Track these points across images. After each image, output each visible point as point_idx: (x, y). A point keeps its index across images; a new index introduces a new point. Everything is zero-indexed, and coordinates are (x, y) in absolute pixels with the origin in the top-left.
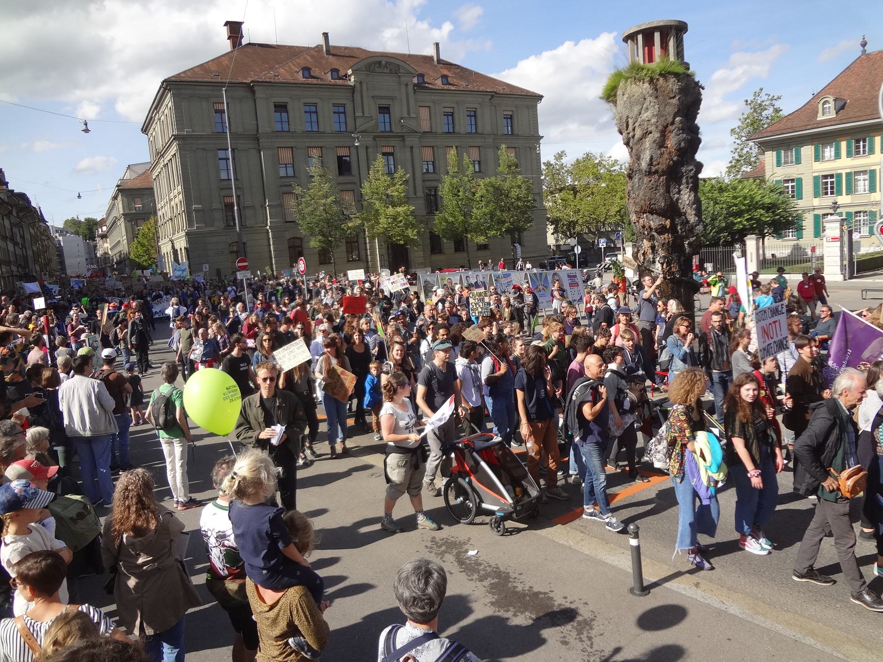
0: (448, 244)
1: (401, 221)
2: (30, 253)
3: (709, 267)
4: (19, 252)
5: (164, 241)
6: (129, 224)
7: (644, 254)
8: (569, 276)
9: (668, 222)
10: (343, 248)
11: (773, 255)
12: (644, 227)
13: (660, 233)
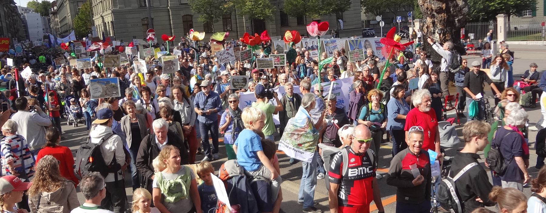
0: (293, 20)
1: (261, 4)
3: (472, 36)
6: (72, 5)
7: (427, 27)
8: (376, 42)
9: (444, 6)
10: (221, 22)
11: (516, 28)
12: (427, 9)
13: (438, 13)
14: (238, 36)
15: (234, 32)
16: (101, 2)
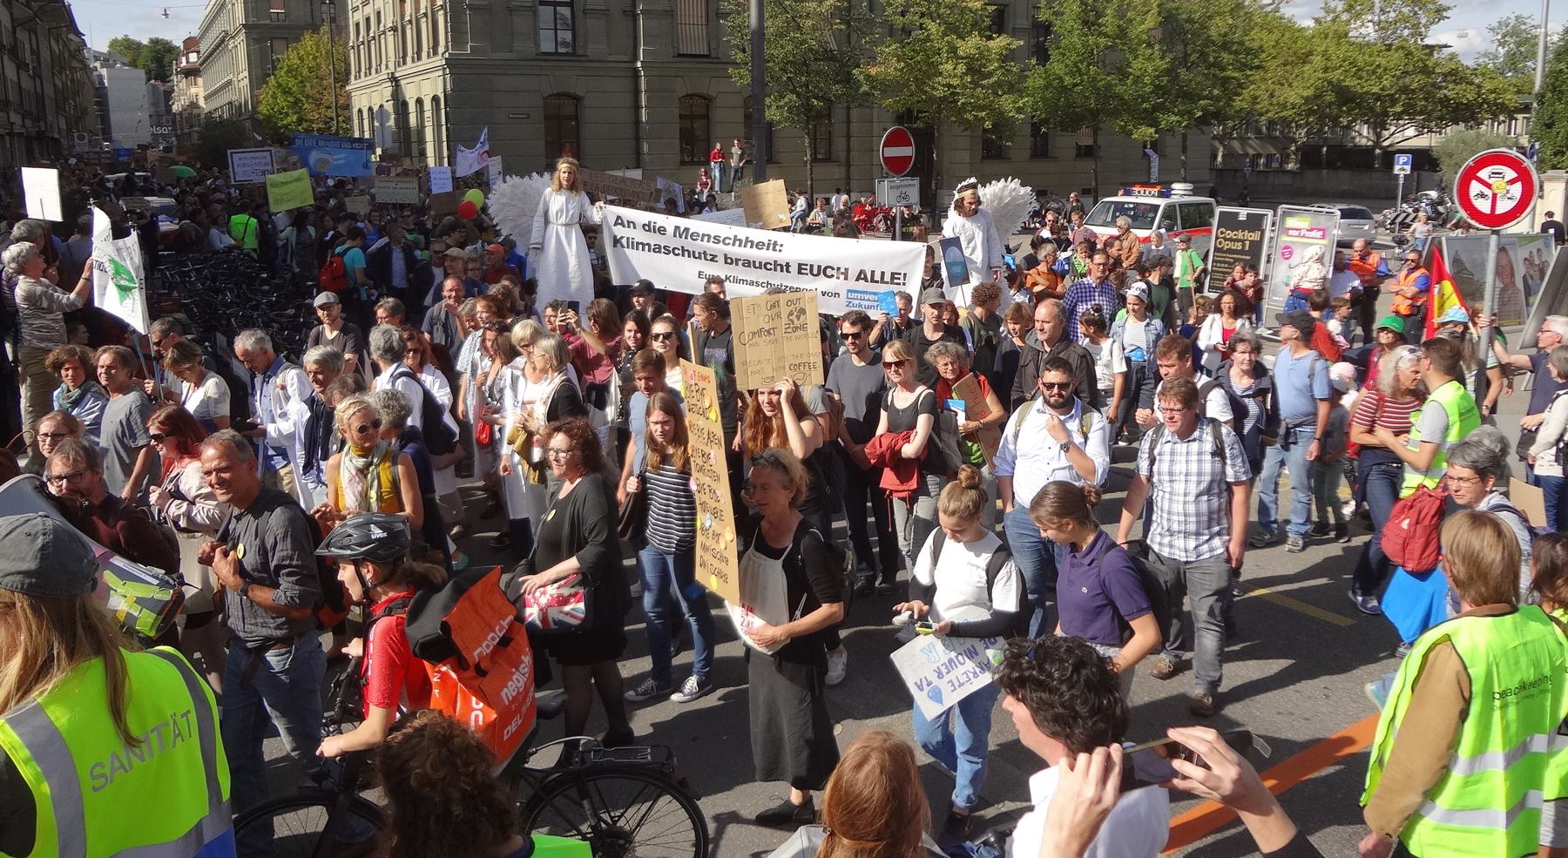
2: (49, 91)
4: (26, 83)
5: (364, 81)
6: (254, 47)
14: (848, 179)
16: (394, 29)
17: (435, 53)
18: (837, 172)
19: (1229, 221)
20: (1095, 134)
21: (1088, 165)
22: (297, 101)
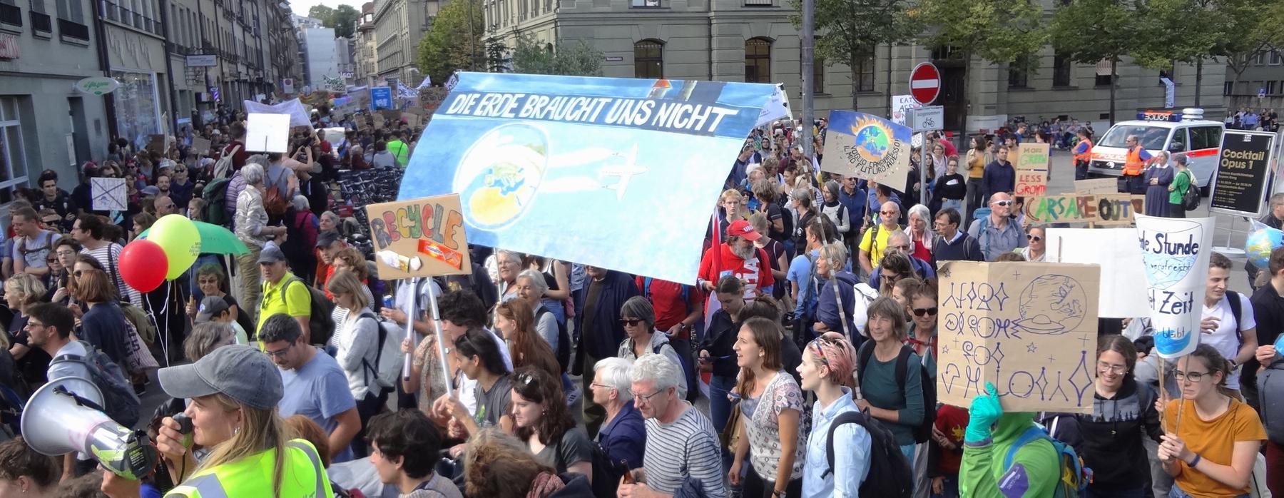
2: (266, 48)
4: (250, 42)
15: (880, 95)
17: (549, 9)
18: (880, 102)
19: (1234, 143)
20: (1114, 65)
21: (1105, 94)
22: (445, 51)
